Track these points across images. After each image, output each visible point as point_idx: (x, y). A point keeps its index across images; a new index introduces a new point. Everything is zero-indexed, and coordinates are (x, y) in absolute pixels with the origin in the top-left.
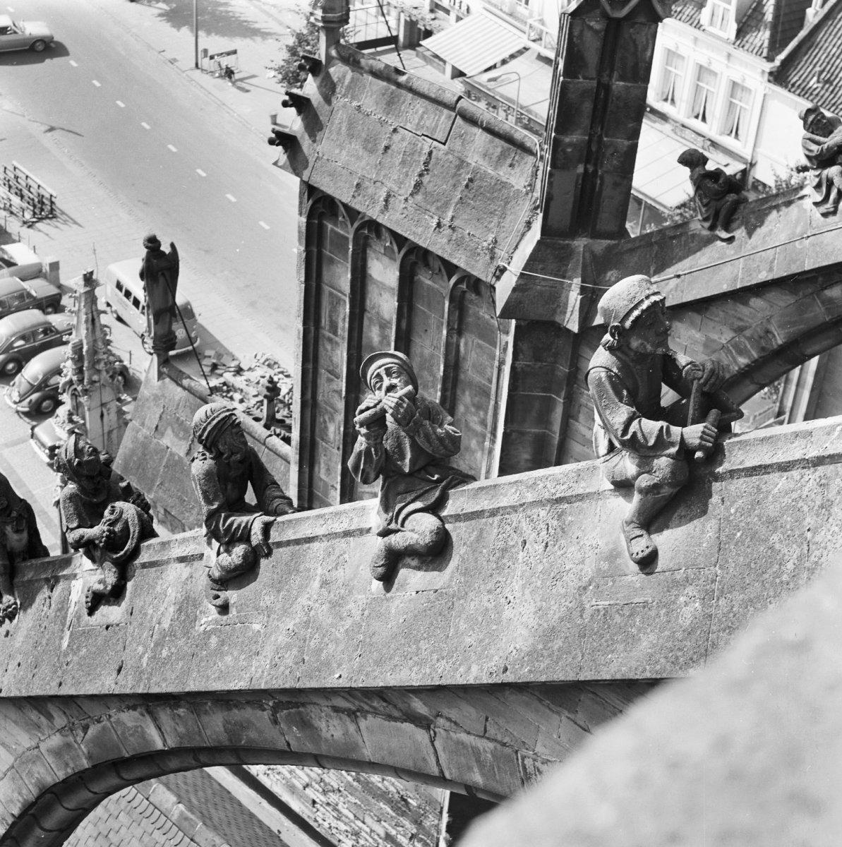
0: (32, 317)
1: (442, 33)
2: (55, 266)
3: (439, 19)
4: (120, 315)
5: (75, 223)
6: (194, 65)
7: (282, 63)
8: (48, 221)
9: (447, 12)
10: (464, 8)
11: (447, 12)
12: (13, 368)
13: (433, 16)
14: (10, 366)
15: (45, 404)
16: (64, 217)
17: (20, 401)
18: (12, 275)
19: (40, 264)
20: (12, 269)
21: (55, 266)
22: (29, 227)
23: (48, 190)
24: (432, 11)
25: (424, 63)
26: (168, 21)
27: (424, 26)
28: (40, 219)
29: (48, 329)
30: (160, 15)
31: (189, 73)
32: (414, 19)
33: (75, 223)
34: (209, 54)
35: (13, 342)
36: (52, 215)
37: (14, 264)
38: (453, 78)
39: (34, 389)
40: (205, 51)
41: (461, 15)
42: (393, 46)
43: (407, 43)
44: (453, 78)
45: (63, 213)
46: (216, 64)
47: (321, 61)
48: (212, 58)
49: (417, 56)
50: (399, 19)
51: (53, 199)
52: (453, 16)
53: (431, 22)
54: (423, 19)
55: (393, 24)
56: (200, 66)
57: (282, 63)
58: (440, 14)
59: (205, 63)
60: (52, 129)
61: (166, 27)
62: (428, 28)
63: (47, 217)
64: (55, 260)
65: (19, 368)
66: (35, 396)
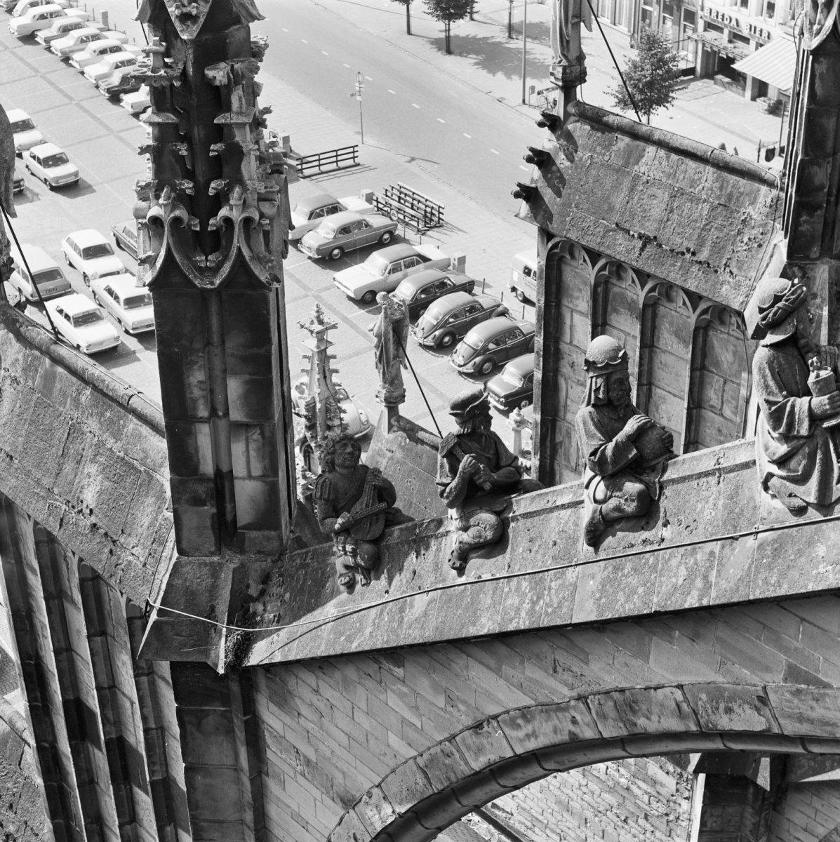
0: (461, 298)
1: (745, 60)
2: (462, 260)
3: (738, 48)
4: (527, 296)
5: (460, 230)
6: (521, 102)
7: (617, 89)
8: (436, 229)
9: (746, 40)
10: (765, 34)
11: (746, 40)
12: (449, 340)
13: (732, 45)
14: (447, 339)
15: (485, 367)
16: (448, 226)
17: (465, 365)
18: (426, 268)
19: (449, 259)
20: (427, 263)
21: (462, 260)
22: (423, 234)
23: (436, 200)
24: (730, 41)
25: (723, 89)
26: (484, 68)
27: (727, 54)
28: (431, 228)
29: (473, 308)
30: (476, 64)
31: (518, 108)
32: (715, 49)
33: (460, 230)
34: (536, 91)
35: (448, 319)
36: (439, 225)
37: (430, 260)
38: (753, 99)
39: (476, 353)
40: (533, 88)
41: (761, 42)
42: (692, 77)
43: (703, 73)
44: (753, 99)
45: (447, 223)
46: (543, 99)
47: (559, 118)
48: (539, 93)
49: (715, 83)
50: (697, 53)
51: (441, 210)
52: (753, 43)
53: (734, 50)
54: (725, 48)
55: (691, 57)
56: (527, 102)
57: (617, 89)
58: (740, 44)
59: (534, 99)
60: (413, 159)
61: (483, 73)
62: (730, 55)
63: (435, 227)
64: (463, 255)
65: (455, 341)
66: (478, 360)
